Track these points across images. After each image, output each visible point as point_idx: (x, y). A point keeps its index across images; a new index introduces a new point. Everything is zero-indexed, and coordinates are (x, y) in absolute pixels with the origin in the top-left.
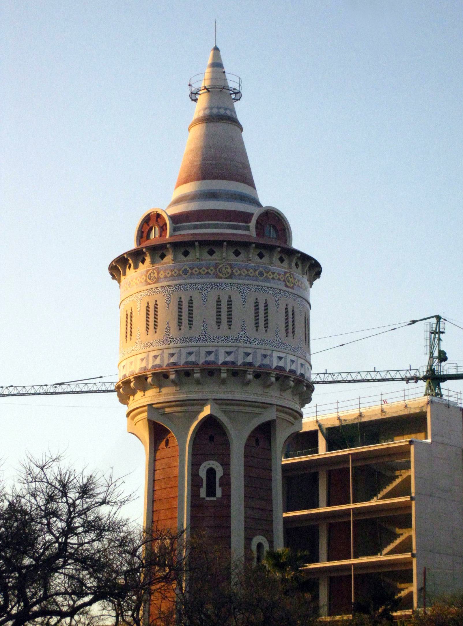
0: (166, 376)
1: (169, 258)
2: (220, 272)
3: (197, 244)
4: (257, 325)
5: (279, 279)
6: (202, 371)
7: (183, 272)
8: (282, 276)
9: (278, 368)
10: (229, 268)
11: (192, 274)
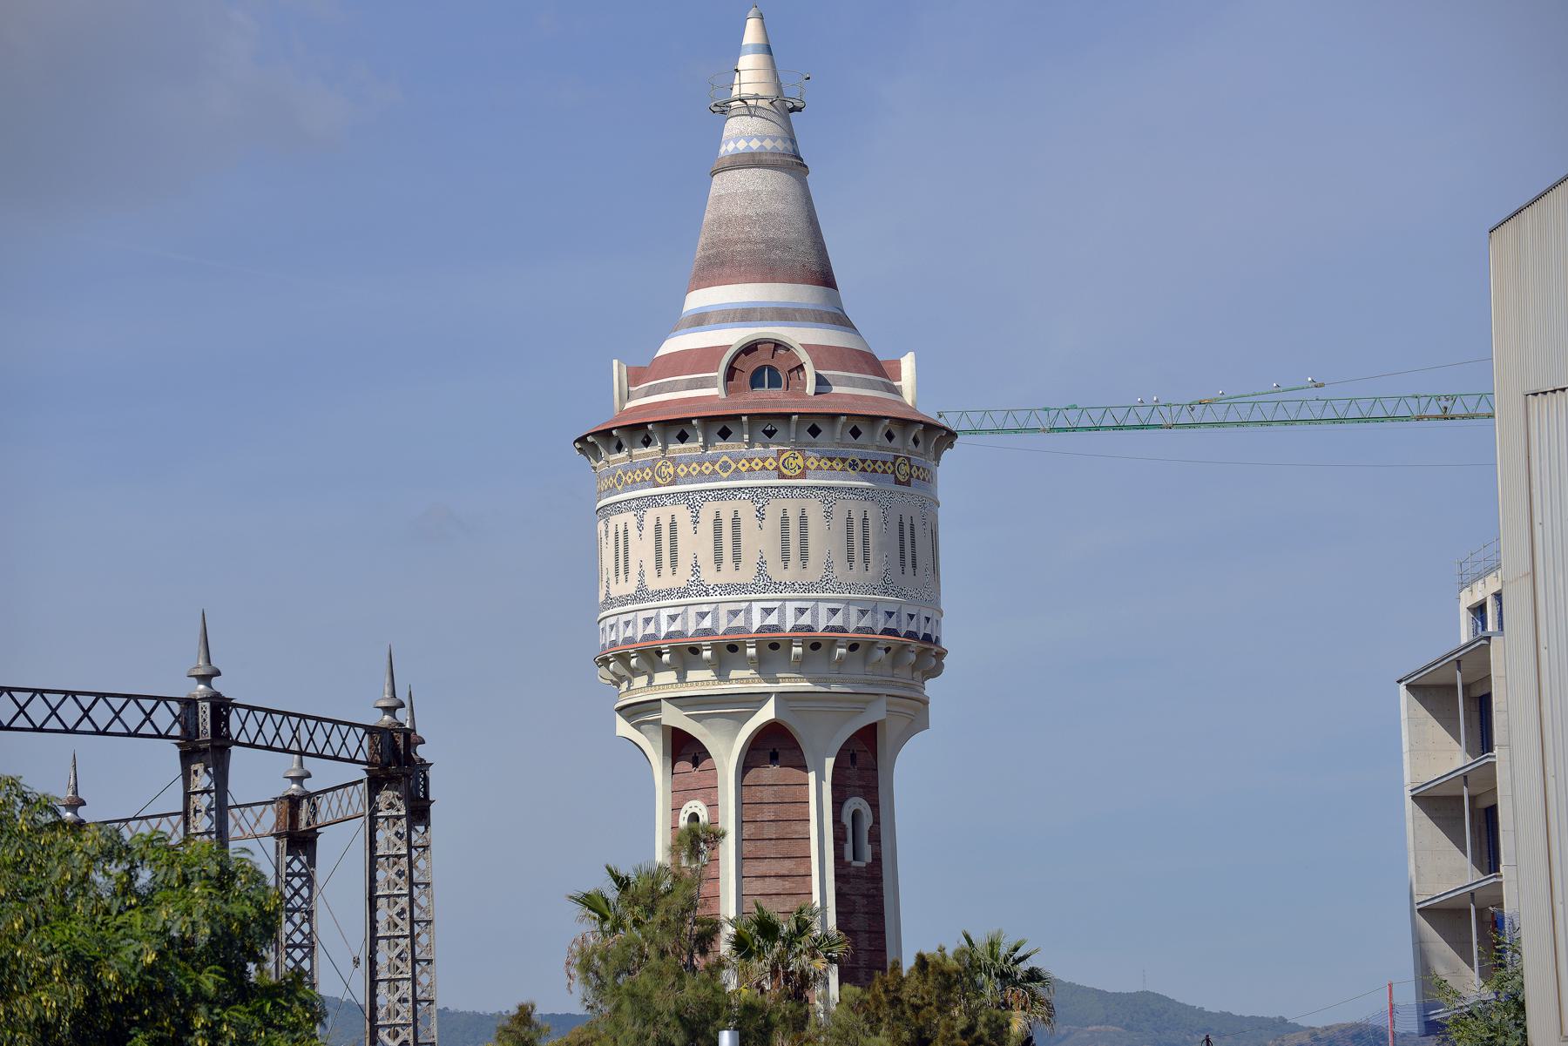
0: (695, 650)
3: (744, 419)
4: (850, 559)
5: (884, 472)
6: (758, 644)
9: (886, 631)
11: (737, 470)
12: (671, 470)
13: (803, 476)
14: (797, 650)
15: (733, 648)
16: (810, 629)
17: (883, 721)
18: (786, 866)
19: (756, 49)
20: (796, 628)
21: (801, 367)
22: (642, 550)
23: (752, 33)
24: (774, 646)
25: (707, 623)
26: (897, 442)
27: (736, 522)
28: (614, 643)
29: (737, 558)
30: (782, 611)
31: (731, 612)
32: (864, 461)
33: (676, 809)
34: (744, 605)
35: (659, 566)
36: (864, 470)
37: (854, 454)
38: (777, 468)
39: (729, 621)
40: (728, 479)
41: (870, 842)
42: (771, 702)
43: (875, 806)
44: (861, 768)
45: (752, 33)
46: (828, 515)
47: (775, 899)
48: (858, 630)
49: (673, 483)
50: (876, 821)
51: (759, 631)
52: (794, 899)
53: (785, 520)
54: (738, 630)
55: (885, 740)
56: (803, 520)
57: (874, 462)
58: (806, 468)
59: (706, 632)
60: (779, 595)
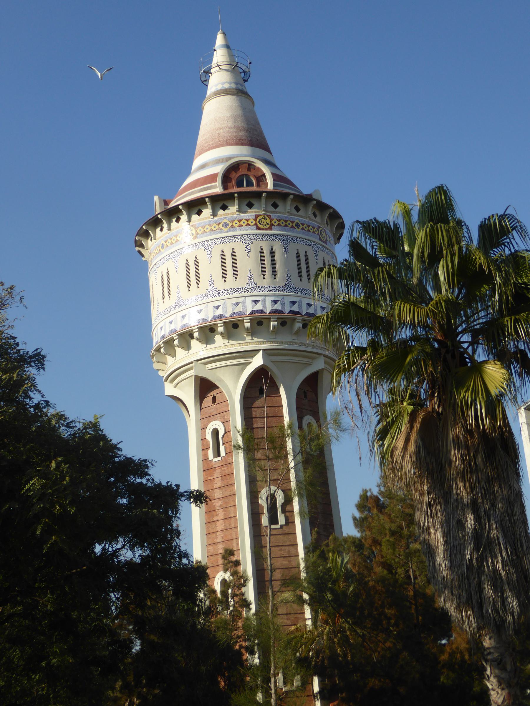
0: (212, 330)
1: (207, 212)
3: (236, 195)
4: (300, 275)
7: (223, 225)
8: (316, 229)
10: (268, 219)
11: (232, 226)
13: (270, 228)
14: (273, 324)
15: (235, 326)
16: (280, 312)
17: (322, 370)
20: (272, 312)
21: (264, 175)
22: (178, 279)
23: (220, 39)
24: (260, 323)
25: (220, 312)
26: (318, 219)
27: (234, 255)
28: (163, 337)
29: (235, 274)
30: (264, 302)
31: (234, 304)
33: (204, 429)
34: (241, 300)
35: (189, 285)
36: (303, 229)
37: (298, 220)
38: (256, 224)
39: (233, 309)
40: (227, 232)
42: (260, 355)
45: (220, 39)
46: (286, 250)
48: (308, 314)
51: (251, 313)
53: (262, 252)
54: (240, 313)
56: (272, 253)
57: (309, 226)
58: (272, 225)
59: (220, 317)
60: (261, 293)
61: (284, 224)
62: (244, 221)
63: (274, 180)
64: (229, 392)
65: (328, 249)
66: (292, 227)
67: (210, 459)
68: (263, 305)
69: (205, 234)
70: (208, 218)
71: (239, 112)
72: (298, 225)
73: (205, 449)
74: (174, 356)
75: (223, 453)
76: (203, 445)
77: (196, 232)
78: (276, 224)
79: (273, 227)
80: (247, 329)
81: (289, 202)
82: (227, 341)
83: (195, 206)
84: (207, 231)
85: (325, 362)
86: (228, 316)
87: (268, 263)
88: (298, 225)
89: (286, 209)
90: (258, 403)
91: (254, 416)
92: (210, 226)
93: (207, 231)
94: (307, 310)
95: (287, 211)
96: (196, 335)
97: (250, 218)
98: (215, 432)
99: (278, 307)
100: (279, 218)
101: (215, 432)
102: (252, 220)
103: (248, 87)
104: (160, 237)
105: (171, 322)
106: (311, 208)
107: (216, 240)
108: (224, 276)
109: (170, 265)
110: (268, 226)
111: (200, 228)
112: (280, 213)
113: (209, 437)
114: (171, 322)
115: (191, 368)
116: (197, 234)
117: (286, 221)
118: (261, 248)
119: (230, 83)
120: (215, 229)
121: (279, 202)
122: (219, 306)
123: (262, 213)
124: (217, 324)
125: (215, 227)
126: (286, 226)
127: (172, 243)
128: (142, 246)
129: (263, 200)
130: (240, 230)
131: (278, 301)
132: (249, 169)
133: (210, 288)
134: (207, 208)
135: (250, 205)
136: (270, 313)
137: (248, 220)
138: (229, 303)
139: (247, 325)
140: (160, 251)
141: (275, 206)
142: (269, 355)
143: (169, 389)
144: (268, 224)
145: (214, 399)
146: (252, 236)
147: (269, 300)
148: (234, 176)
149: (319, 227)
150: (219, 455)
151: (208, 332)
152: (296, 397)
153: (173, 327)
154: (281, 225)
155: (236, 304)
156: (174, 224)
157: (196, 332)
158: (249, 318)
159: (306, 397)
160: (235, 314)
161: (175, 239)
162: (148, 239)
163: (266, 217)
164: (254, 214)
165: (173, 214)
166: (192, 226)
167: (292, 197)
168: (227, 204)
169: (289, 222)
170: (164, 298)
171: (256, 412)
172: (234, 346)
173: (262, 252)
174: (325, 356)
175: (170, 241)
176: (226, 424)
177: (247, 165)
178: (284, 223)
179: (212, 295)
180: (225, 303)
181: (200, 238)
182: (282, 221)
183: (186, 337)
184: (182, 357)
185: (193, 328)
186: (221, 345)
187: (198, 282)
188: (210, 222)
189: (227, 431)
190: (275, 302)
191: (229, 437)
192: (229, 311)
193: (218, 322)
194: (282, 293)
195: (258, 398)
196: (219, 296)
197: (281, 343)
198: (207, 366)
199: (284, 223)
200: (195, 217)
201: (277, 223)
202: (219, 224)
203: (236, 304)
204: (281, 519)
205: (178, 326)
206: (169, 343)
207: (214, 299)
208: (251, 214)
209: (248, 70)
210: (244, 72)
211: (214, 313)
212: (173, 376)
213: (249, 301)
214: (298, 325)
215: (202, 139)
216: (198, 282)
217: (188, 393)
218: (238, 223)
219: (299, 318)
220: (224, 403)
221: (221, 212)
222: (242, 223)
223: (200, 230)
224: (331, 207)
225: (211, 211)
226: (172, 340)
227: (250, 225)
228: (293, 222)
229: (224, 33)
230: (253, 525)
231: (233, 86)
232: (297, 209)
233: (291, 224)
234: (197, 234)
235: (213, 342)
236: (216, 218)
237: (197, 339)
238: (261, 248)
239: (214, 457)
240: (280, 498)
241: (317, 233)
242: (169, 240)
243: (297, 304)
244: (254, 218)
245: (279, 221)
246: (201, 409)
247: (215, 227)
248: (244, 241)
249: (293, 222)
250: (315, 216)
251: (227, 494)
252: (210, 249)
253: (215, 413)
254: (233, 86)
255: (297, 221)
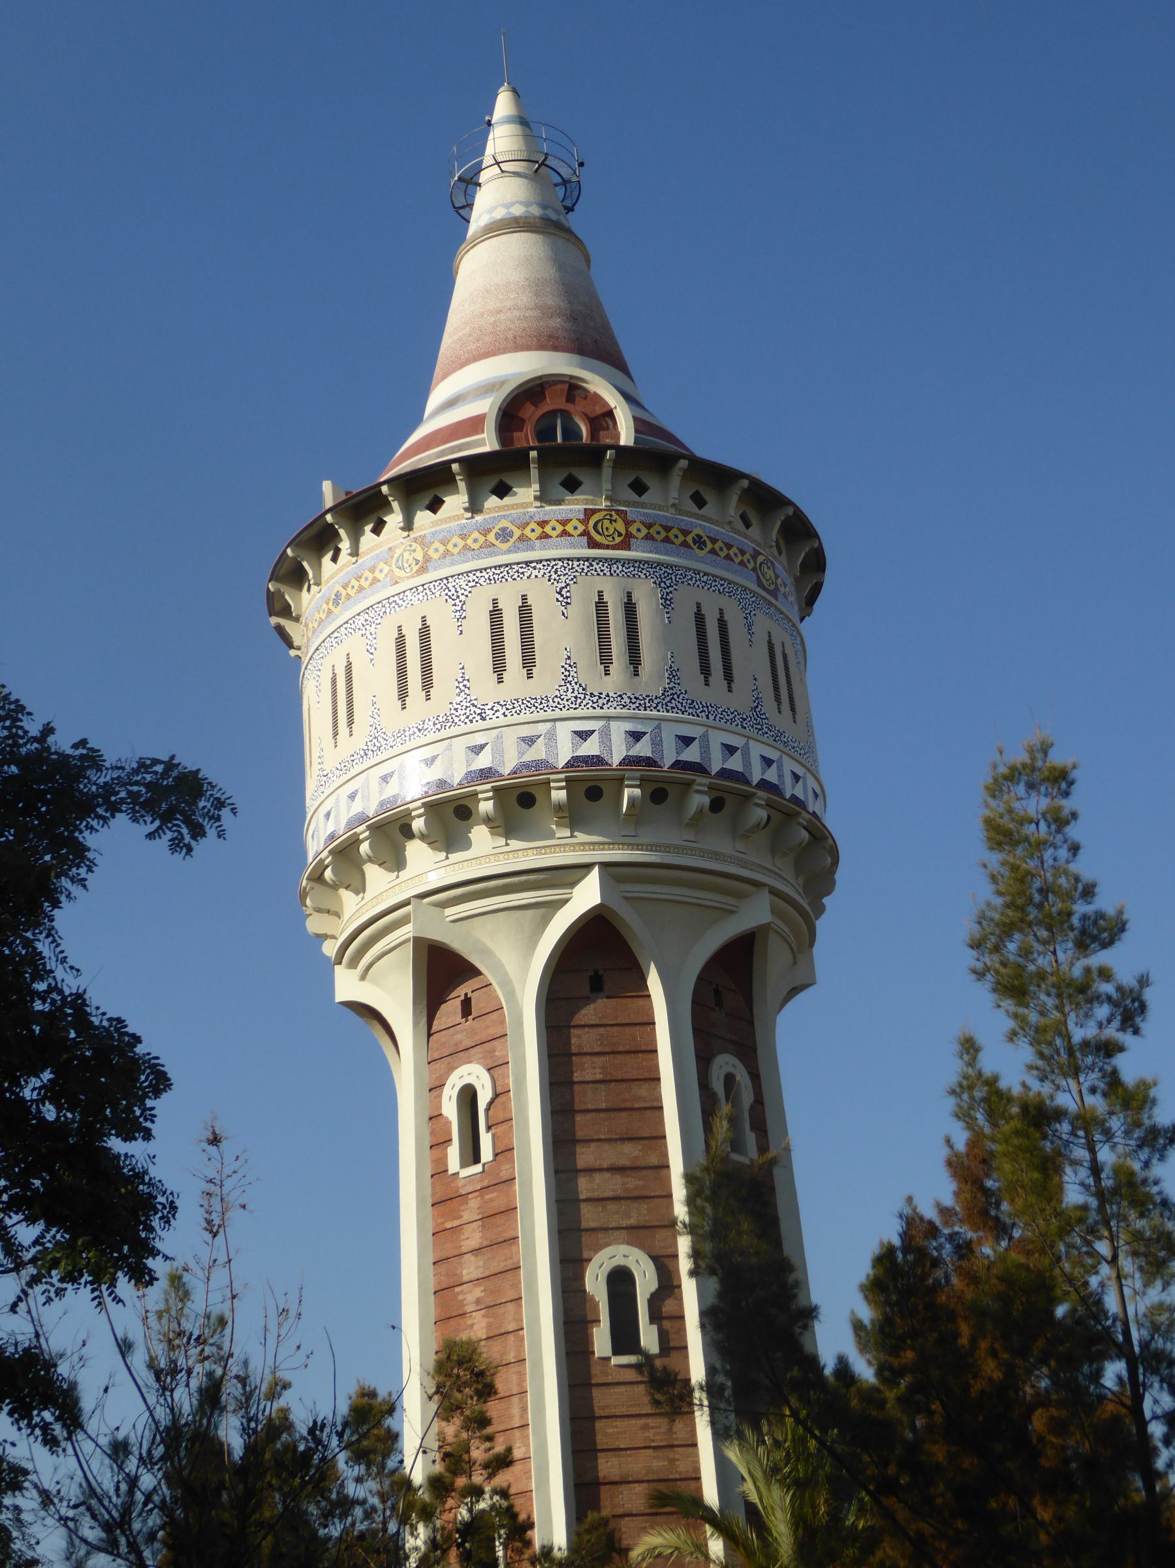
1: (455, 502)
2: (598, 532)
4: (705, 670)
7: (497, 536)
8: (747, 556)
10: (619, 520)
12: (419, 555)
13: (625, 545)
16: (649, 762)
17: (765, 929)
18: (628, 1153)
19: (509, 120)
20: (628, 761)
21: (610, 414)
22: (376, 679)
23: (503, 105)
25: (484, 761)
26: (755, 531)
27: (525, 612)
28: (332, 837)
29: (528, 661)
30: (606, 734)
31: (524, 739)
32: (714, 541)
33: (437, 1088)
34: (543, 728)
35: (403, 694)
37: (700, 527)
38: (585, 533)
39: (521, 754)
40: (509, 551)
41: (753, 1128)
42: (593, 880)
43: (755, 1076)
44: (731, 1007)
45: (503, 105)
46: (667, 602)
47: (611, 1206)
48: (724, 773)
49: (423, 570)
50: (759, 1102)
51: (569, 765)
52: (644, 1207)
53: (601, 606)
54: (539, 765)
55: (774, 963)
56: (630, 610)
57: (729, 547)
58: (629, 535)
59: (486, 774)
61: (662, 534)
62: (553, 523)
63: (636, 431)
64: (507, 983)
65: (782, 613)
66: (685, 544)
67: (450, 1172)
68: (602, 742)
69: (448, 560)
70: (458, 517)
71: (550, 272)
72: (699, 542)
73: (440, 1144)
74: (360, 889)
75: (487, 1154)
76: (432, 1133)
77: (426, 555)
78: (640, 535)
79: (633, 541)
80: (559, 807)
81: (676, 480)
82: (502, 841)
83: (424, 487)
84: (455, 551)
85: (774, 910)
86: (506, 771)
87: (616, 635)
88: (699, 542)
89: (667, 497)
90: (588, 1013)
91: (574, 1049)
92: (464, 537)
93: (455, 551)
94: (724, 761)
95: (671, 501)
96: (418, 825)
97: (570, 516)
98: (468, 1096)
99: (643, 749)
100: (649, 520)
101: (468, 1096)
102: (575, 523)
103: (573, 221)
104: (331, 577)
105: (352, 797)
106: (735, 498)
107: (478, 574)
108: (499, 666)
109: (354, 645)
110: (618, 540)
111: (437, 545)
112: (653, 506)
113: (450, 1109)
114: (352, 797)
115: (404, 921)
116: (427, 559)
117: (667, 529)
118: (600, 594)
119: (527, 204)
120: (476, 546)
121: (649, 480)
122: (482, 747)
123: (604, 504)
124: (476, 794)
125: (475, 541)
126: (667, 540)
127: (361, 588)
128: (286, 611)
129: (607, 471)
130: (544, 548)
131: (645, 733)
132: (570, 399)
133: (458, 699)
134: (456, 491)
135: (572, 485)
136: (620, 764)
137: (564, 523)
138: (511, 738)
139: (559, 795)
140: (330, 612)
141: (639, 488)
142: (619, 880)
143: (347, 986)
144: (620, 535)
145: (466, 1006)
146: (576, 563)
147: (618, 730)
148: (532, 414)
149: (756, 554)
150: (476, 1159)
151: (450, 817)
152: (694, 1002)
153: (357, 807)
154: (653, 539)
155: (530, 741)
156: (368, 538)
157: (419, 816)
158: (563, 776)
159: (719, 1003)
160: (526, 766)
161: (370, 576)
162: (301, 589)
163: (615, 516)
164: (582, 507)
165: (364, 509)
166: (415, 540)
167: (683, 463)
168: (509, 483)
169: (675, 531)
170: (335, 734)
171: (581, 1040)
172: (523, 855)
173: (601, 606)
174: (774, 892)
175: (356, 584)
176: (497, 1072)
177: (566, 386)
178: (663, 534)
179: (463, 718)
180: (499, 737)
181: (436, 569)
182: (657, 528)
183: (391, 833)
184: (382, 887)
185: (411, 806)
186: (486, 851)
187: (427, 684)
188: (463, 527)
189: (499, 1090)
190: (636, 736)
191: (506, 1107)
192: (508, 759)
193: (479, 788)
194: (655, 712)
195: (588, 1000)
196: (483, 719)
197: (651, 847)
198: (449, 911)
199: (663, 534)
200: (423, 518)
201: (644, 531)
202: (485, 532)
203: (530, 741)
204: (648, 1337)
205: (370, 805)
206: (345, 853)
207: (470, 727)
208: (573, 507)
209: (574, 179)
210: (565, 182)
211: (469, 764)
212: (356, 947)
213: (565, 731)
214: (699, 800)
215: (450, 341)
216: (427, 684)
217: (392, 991)
218: (539, 530)
219: (702, 781)
220: (494, 1016)
221: (493, 501)
222: (548, 529)
223: (437, 550)
224: (789, 503)
225: (465, 498)
226: (355, 842)
227: (570, 535)
228: (686, 533)
229: (514, 91)
230: (568, 1354)
231: (536, 211)
232: (700, 501)
233: (681, 538)
234: (427, 559)
235: (466, 845)
236: (479, 518)
237: (423, 837)
238: (600, 594)
239: (464, 1164)
240: (645, 1282)
241: (751, 566)
242: (354, 582)
243: (695, 745)
244: (582, 516)
245: (649, 526)
246: (429, 1035)
247: (475, 541)
248: (554, 576)
249: (686, 533)
250: (748, 525)
251: (497, 1266)
252: (463, 598)
253: (468, 1043)
254: (536, 211)
255: (697, 531)
